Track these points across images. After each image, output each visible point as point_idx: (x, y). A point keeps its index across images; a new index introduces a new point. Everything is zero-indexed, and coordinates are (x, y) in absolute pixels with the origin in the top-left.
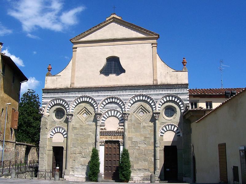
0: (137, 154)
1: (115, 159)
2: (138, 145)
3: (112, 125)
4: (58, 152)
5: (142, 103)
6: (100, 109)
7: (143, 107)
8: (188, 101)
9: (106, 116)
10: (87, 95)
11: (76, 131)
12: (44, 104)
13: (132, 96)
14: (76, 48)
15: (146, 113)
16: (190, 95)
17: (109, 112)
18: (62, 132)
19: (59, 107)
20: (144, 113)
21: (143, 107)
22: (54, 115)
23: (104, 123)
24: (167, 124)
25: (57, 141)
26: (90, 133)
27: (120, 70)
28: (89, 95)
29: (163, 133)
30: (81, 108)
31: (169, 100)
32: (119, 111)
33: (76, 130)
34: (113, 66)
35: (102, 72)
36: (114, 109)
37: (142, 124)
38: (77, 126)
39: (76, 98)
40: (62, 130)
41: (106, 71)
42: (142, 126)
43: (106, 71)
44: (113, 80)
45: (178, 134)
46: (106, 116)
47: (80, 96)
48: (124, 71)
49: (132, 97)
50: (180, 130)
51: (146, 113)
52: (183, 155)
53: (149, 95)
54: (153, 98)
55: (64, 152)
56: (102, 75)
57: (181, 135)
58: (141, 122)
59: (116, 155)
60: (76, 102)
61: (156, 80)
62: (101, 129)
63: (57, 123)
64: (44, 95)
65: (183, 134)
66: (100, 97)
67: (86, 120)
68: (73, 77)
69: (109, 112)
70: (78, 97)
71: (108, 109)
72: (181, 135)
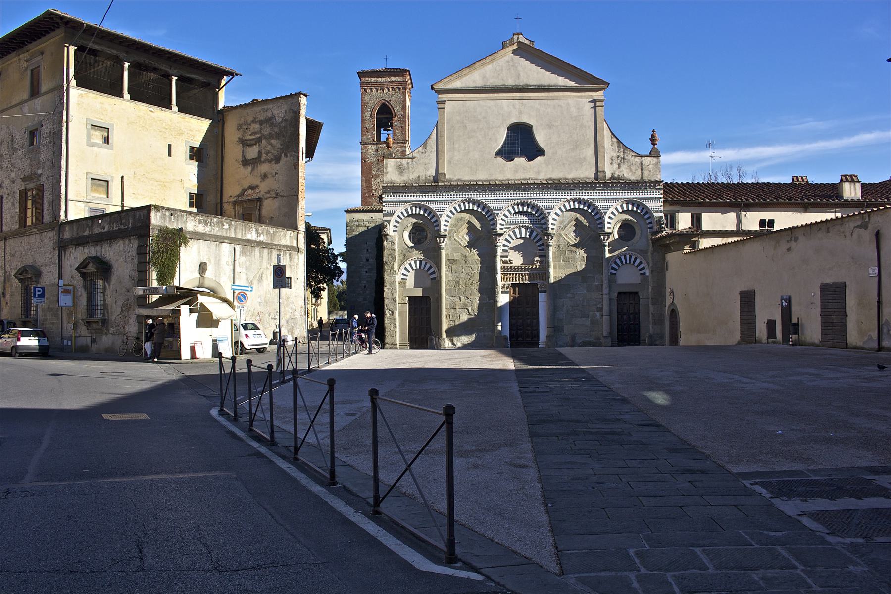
8: (661, 212)
14: (444, 102)
16: (664, 202)
17: (517, 230)
27: (533, 151)
29: (616, 270)
31: (628, 210)
34: (521, 142)
35: (499, 154)
41: (507, 153)
43: (507, 153)
44: (520, 169)
48: (541, 152)
52: (651, 308)
56: (500, 159)
57: (647, 274)
65: (652, 272)
69: (517, 230)
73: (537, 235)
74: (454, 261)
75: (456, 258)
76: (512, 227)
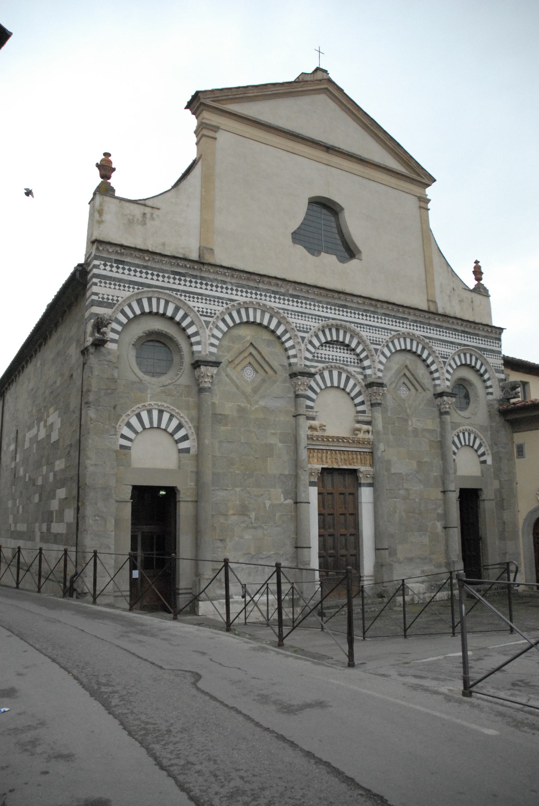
0: (404, 514)
1: (343, 531)
2: (406, 486)
3: (335, 415)
4: (154, 507)
5: (409, 359)
6: (306, 359)
7: (409, 370)
9: (318, 384)
10: (265, 302)
11: (223, 428)
12: (100, 304)
13: (391, 333)
15: (417, 390)
18: (170, 430)
19: (157, 325)
20: (409, 390)
21: (409, 370)
22: (132, 354)
23: (312, 408)
24: (461, 428)
25: (148, 464)
26: (274, 440)
28: (273, 305)
30: (238, 347)
32: (354, 376)
33: (226, 425)
35: (298, 237)
36: (342, 366)
37: (410, 423)
38: (228, 408)
39: (229, 306)
40: (170, 420)
42: (410, 429)
45: (482, 459)
46: (318, 384)
47: (242, 299)
49: (390, 336)
50: (488, 448)
51: (417, 390)
53: (427, 341)
54: (437, 352)
55: (184, 510)
56: (300, 250)
57: (489, 462)
58: (408, 415)
59: (348, 516)
60: (224, 320)
61: (434, 302)
62: (311, 428)
63: (149, 391)
64: (102, 267)
65: (493, 460)
66: (306, 318)
67: (255, 391)
68: (206, 225)
70: (235, 303)
71: (328, 362)
72: (489, 462)
73: (355, 386)
74: (225, 416)
75: (226, 413)
76: (321, 365)
